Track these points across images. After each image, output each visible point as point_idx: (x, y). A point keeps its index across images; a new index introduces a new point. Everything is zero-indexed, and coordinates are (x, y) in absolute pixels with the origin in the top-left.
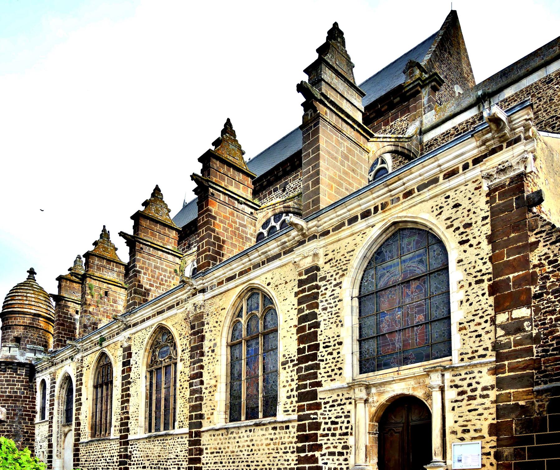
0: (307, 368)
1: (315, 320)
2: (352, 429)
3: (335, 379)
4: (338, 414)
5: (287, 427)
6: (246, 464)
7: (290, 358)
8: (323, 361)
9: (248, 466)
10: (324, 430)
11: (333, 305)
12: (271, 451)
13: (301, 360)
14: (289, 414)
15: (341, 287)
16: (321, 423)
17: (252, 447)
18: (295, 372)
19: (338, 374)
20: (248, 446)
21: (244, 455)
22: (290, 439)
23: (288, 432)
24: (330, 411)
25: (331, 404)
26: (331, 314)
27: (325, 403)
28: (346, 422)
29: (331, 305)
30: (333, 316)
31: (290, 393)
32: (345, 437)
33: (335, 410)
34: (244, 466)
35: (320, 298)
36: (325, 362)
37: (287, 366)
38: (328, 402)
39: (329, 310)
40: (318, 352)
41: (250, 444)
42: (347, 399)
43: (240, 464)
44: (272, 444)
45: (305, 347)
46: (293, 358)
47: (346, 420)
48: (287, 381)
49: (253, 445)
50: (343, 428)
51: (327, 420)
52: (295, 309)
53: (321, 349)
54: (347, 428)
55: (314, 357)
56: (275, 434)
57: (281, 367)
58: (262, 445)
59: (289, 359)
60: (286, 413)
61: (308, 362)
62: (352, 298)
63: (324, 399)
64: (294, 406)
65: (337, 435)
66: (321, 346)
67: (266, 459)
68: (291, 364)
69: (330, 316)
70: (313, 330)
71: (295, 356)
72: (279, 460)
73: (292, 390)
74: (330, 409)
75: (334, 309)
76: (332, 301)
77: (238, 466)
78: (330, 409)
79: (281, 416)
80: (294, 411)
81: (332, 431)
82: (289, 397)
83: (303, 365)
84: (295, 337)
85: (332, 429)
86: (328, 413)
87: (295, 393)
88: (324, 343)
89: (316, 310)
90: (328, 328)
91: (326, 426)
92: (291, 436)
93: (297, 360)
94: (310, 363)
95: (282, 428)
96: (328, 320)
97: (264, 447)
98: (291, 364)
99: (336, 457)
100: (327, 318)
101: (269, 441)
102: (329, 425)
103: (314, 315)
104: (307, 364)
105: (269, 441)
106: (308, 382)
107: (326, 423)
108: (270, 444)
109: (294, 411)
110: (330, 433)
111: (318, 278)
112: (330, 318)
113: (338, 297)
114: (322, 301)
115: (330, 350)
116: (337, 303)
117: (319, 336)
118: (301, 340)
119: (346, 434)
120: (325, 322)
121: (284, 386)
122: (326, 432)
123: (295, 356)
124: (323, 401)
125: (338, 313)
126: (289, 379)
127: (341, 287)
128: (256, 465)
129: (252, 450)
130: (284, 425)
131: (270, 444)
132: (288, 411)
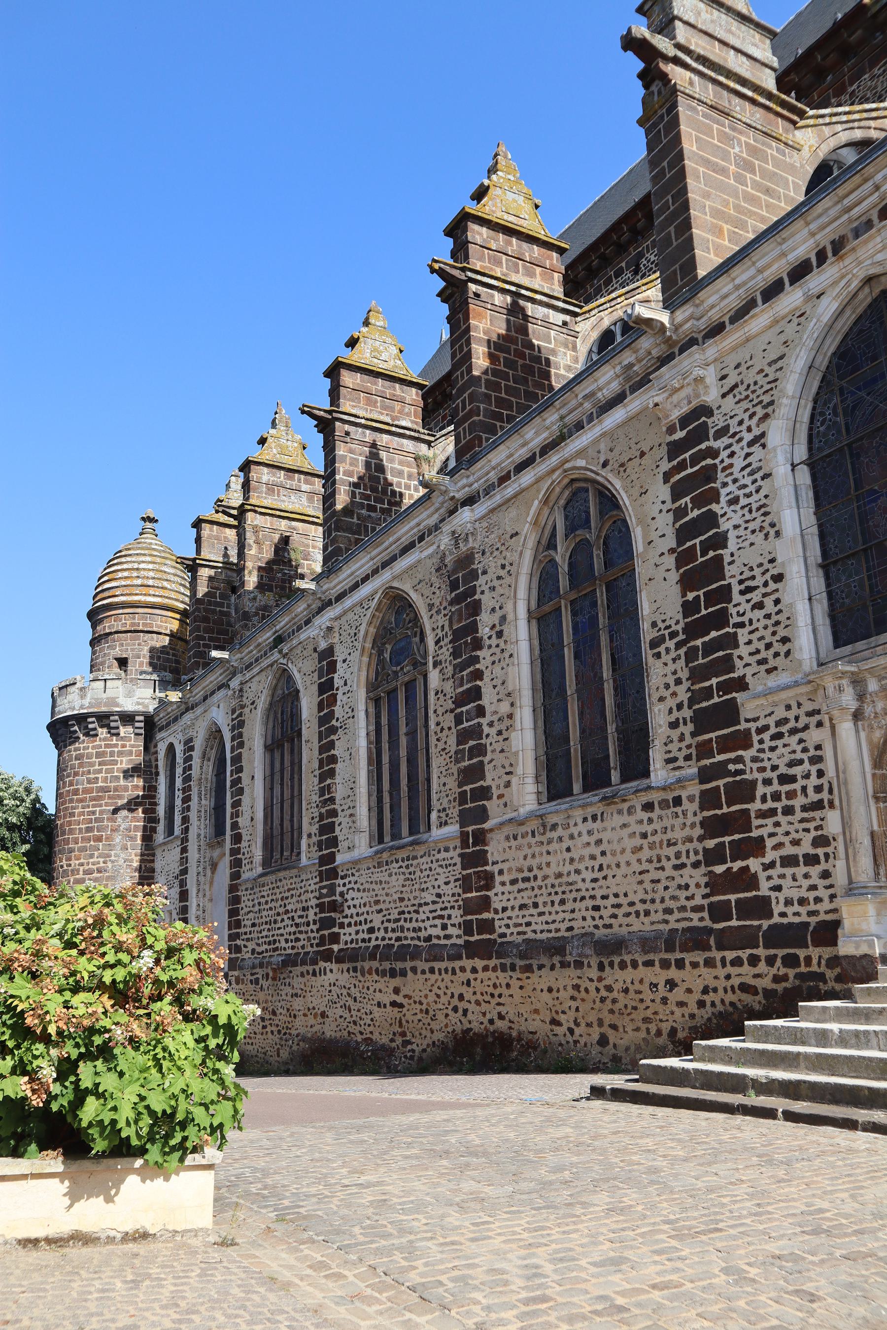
0: (709, 648)
1: (715, 530)
2: (831, 791)
3: (775, 668)
4: (793, 756)
5: (678, 801)
6: (590, 903)
7: (667, 628)
8: (742, 625)
9: (596, 908)
10: (764, 799)
11: (752, 488)
12: (645, 866)
13: (693, 630)
14: (679, 768)
15: (764, 446)
16: (754, 783)
17: (600, 860)
18: (683, 661)
19: (782, 654)
20: (593, 857)
21: (584, 880)
22: (687, 832)
23: (680, 814)
24: (773, 749)
25: (773, 730)
26: (750, 511)
27: (760, 731)
28: (814, 774)
29: (747, 491)
30: (754, 514)
31: (676, 714)
32: (817, 814)
33: (785, 746)
34: (587, 909)
35: (721, 476)
36: (749, 628)
37: (662, 649)
38: (766, 728)
39: (743, 501)
40: (730, 606)
41: (597, 851)
42: (810, 714)
43: (578, 905)
44: (646, 846)
45: (698, 596)
46: (674, 628)
47: (814, 770)
48: (667, 686)
49: (603, 853)
50: (810, 790)
51: (769, 774)
52: (668, 511)
53: (736, 597)
54: (818, 789)
55: (721, 619)
56: (650, 820)
57: (650, 653)
58: (623, 851)
59: (666, 632)
60: (671, 766)
61: (708, 634)
62: (794, 466)
63: (755, 720)
64: (689, 747)
65: (798, 809)
66: (736, 589)
67: (635, 887)
68: (672, 644)
69: (748, 517)
70: (711, 554)
71: (677, 623)
72: (666, 888)
73: (680, 707)
74: (773, 744)
75: (755, 497)
76: (748, 481)
77: (573, 911)
78: (773, 744)
79: (659, 774)
80: (688, 758)
81: (785, 802)
82: (674, 725)
83: (699, 642)
84: (674, 576)
85: (783, 796)
86: (768, 754)
87: (687, 713)
88: (741, 582)
89: (714, 507)
90: (747, 543)
91: (768, 790)
92: (688, 824)
93: (684, 631)
94: (714, 634)
95: (664, 804)
96: (744, 525)
97: (628, 856)
98: (672, 644)
99: (802, 870)
100: (740, 521)
101: (638, 841)
102: (776, 786)
103: (711, 519)
104: (707, 639)
105: (638, 841)
106: (714, 681)
107: (767, 782)
108: (641, 848)
109: (688, 758)
110: (778, 805)
111: (711, 432)
112: (747, 522)
113: (760, 468)
114: (725, 485)
115: (756, 596)
116: (760, 483)
117: (727, 567)
118: (687, 583)
119: (818, 805)
120: (736, 533)
121: (661, 699)
122: (770, 804)
123: (677, 623)
124: (753, 726)
125: (764, 506)
126: (671, 680)
127: (764, 446)
128: (613, 906)
129: (601, 868)
130: (670, 796)
131: (641, 848)
132: (675, 759)
